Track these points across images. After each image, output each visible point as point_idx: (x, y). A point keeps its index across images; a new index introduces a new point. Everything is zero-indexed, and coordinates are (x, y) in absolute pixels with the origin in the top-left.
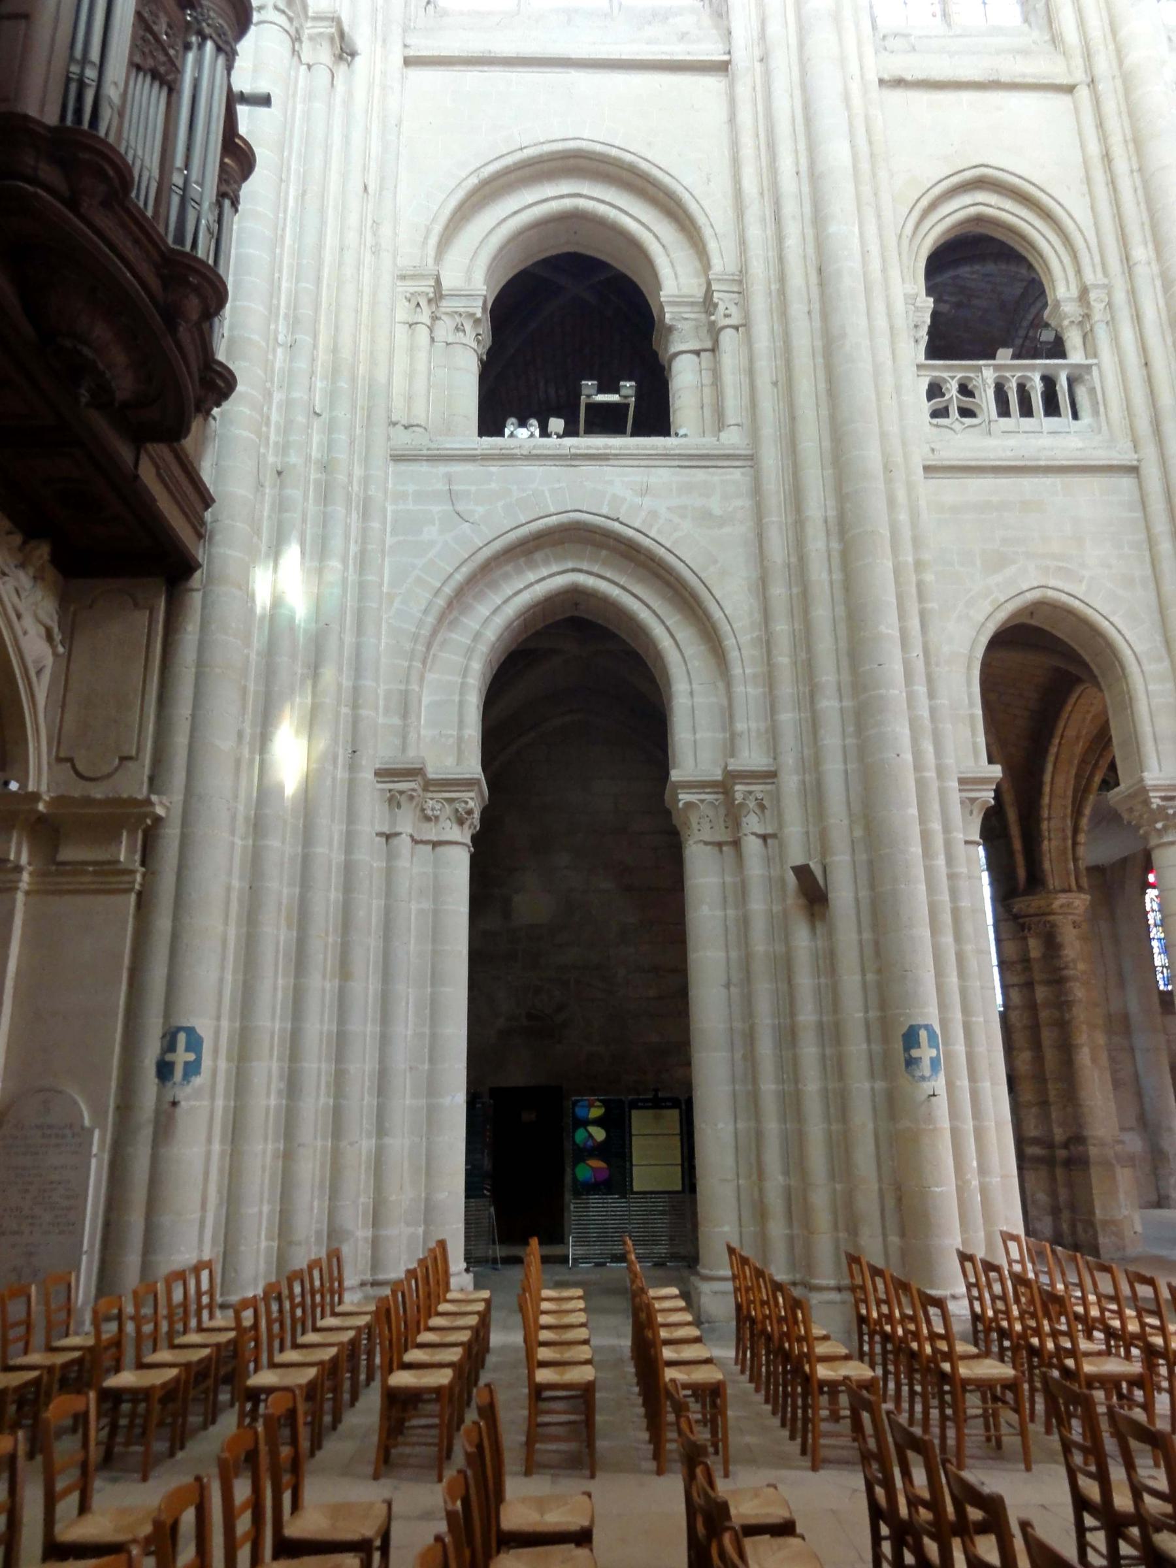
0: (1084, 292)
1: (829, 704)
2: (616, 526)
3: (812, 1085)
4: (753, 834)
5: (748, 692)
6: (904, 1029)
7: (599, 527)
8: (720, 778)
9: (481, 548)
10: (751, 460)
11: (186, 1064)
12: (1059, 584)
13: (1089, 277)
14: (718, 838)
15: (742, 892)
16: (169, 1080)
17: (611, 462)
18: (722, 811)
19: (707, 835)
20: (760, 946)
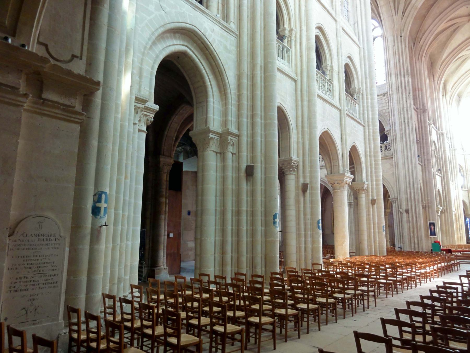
0: (291, 30)
1: (258, 120)
2: (205, 38)
3: (244, 227)
4: (231, 152)
5: (232, 109)
6: (274, 214)
7: (200, 36)
8: (221, 132)
9: (167, 24)
10: (239, 37)
11: (105, 208)
12: (283, 104)
13: (293, 26)
14: (216, 151)
15: (224, 168)
16: (98, 215)
17: (205, 15)
18: (218, 143)
19: (214, 148)
20: (230, 185)
